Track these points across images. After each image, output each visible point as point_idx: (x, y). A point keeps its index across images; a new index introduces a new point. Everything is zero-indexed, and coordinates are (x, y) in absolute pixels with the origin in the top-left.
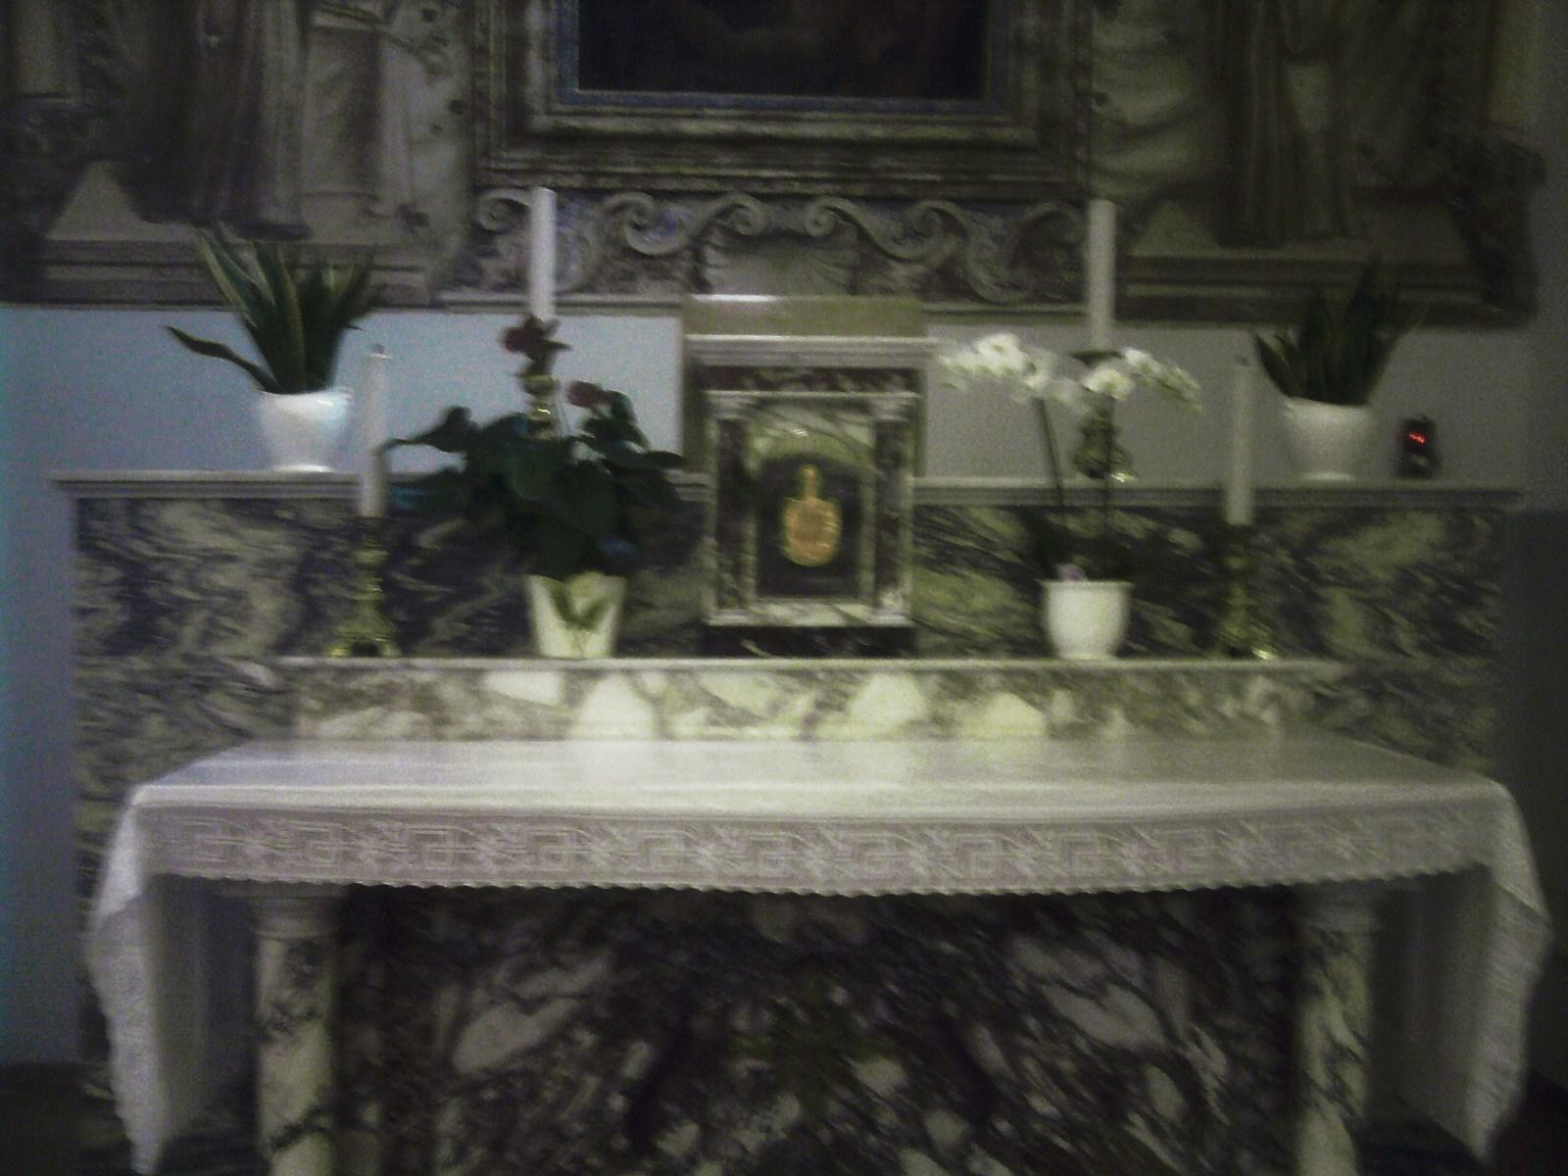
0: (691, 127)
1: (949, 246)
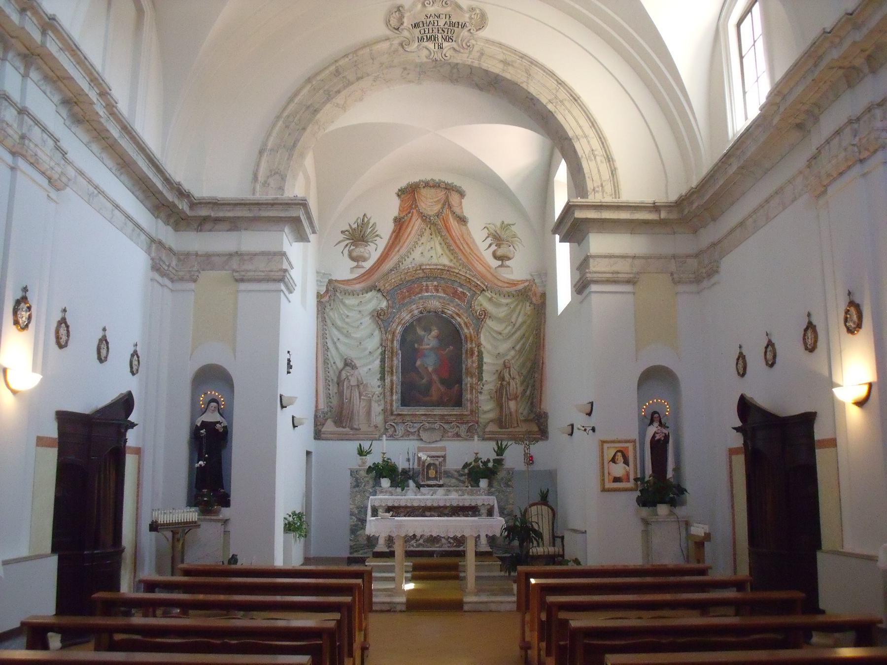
0: (417, 413)
1: (458, 429)
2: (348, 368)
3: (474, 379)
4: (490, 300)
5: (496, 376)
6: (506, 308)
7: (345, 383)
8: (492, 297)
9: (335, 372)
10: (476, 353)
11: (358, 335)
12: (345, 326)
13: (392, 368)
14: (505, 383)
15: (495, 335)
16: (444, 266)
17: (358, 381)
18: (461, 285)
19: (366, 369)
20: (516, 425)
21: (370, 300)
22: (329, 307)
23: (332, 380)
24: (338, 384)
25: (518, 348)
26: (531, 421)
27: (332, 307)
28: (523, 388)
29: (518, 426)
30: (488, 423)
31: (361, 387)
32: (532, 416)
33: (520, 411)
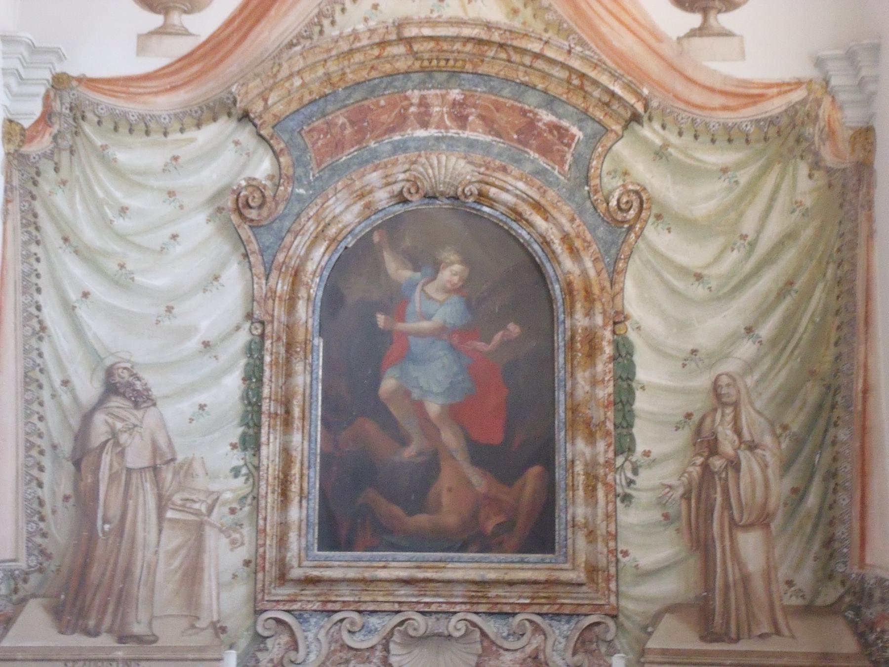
0: (382, 574)
1: (537, 641)
2: (116, 402)
3: (601, 446)
4: (660, 154)
5: (686, 434)
6: (719, 185)
7: (106, 459)
8: (666, 145)
9: (64, 418)
10: (608, 350)
11: (160, 281)
12: (116, 247)
13: (287, 404)
14: (717, 463)
15: (679, 284)
16: (489, 26)
17: (155, 449)
18: (550, 102)
19: (187, 406)
20: (766, 628)
21: (210, 154)
22: (52, 174)
23: (54, 447)
24: (77, 464)
25: (766, 331)
26: (832, 610)
27: (64, 174)
28: (788, 483)
29: (778, 632)
30: (657, 618)
31: (168, 475)
32: (831, 594)
33: (783, 572)
